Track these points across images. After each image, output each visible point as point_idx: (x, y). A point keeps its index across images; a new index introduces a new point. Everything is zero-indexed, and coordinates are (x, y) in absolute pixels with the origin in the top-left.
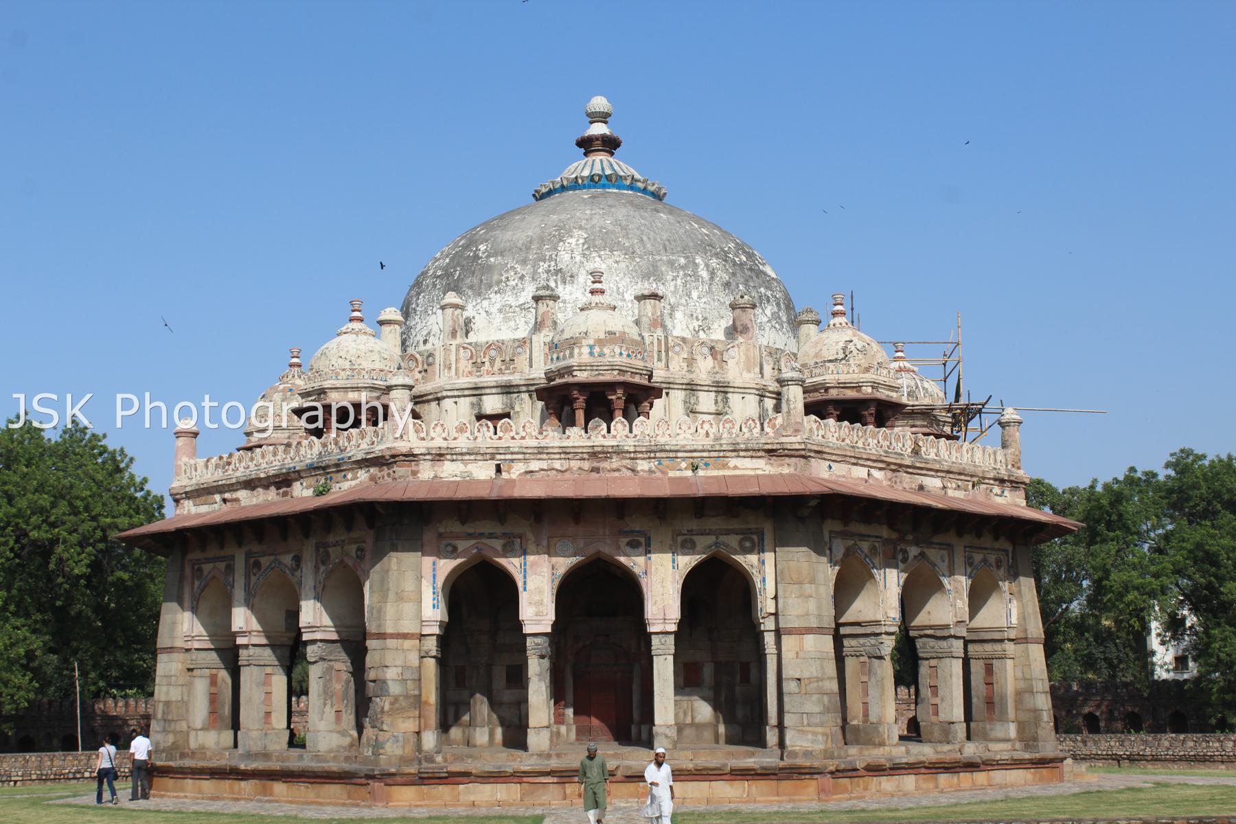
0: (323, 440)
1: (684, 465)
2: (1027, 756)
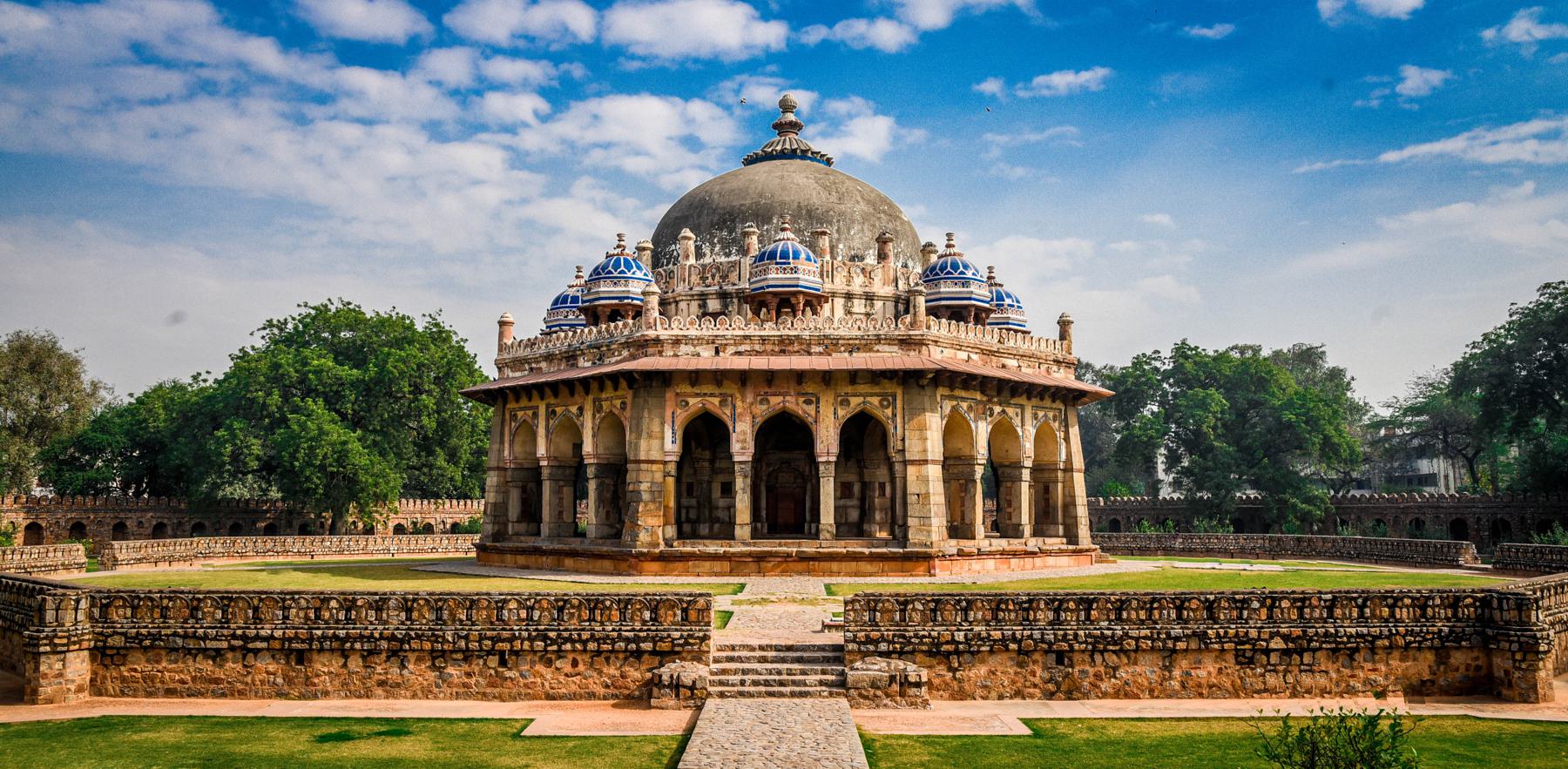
1: (843, 349)
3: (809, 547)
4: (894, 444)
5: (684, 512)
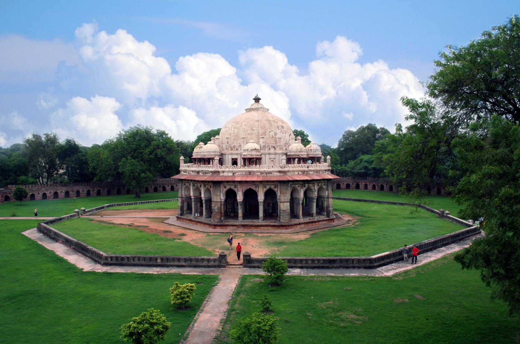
2: (327, 218)
3: (256, 222)
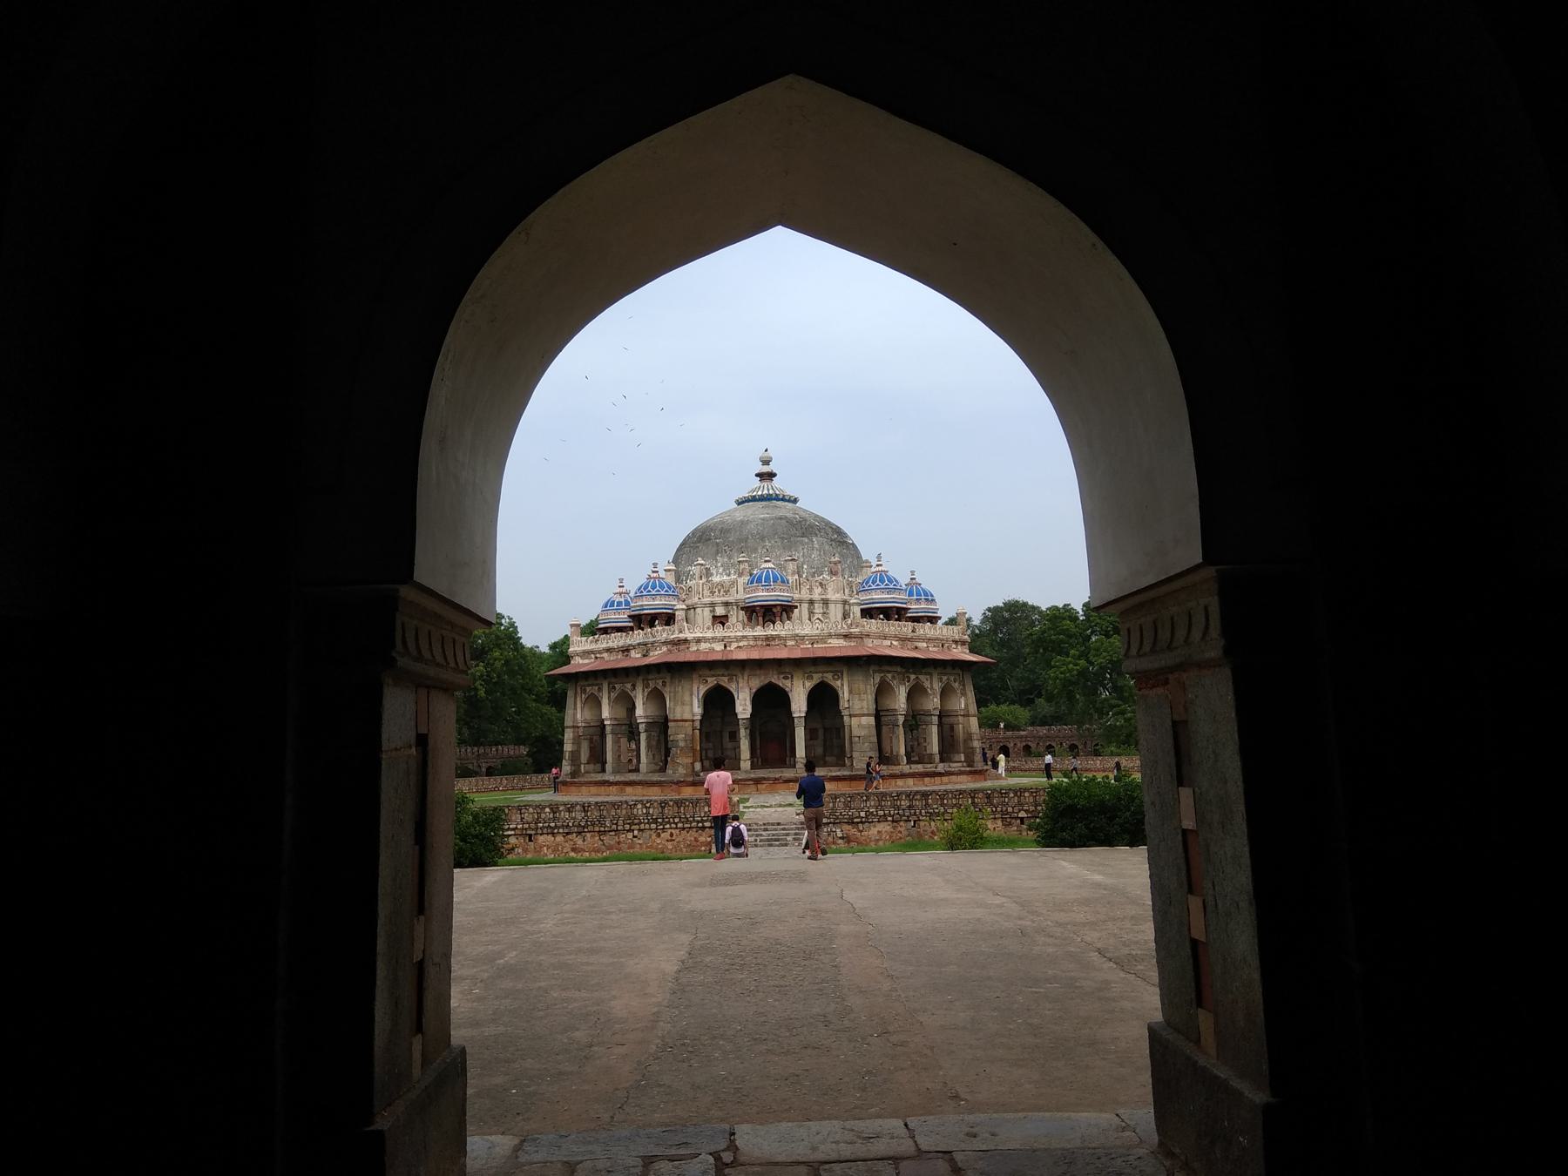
0: (645, 631)
2: (968, 769)
3: (788, 773)
4: (843, 704)
5: (704, 752)
